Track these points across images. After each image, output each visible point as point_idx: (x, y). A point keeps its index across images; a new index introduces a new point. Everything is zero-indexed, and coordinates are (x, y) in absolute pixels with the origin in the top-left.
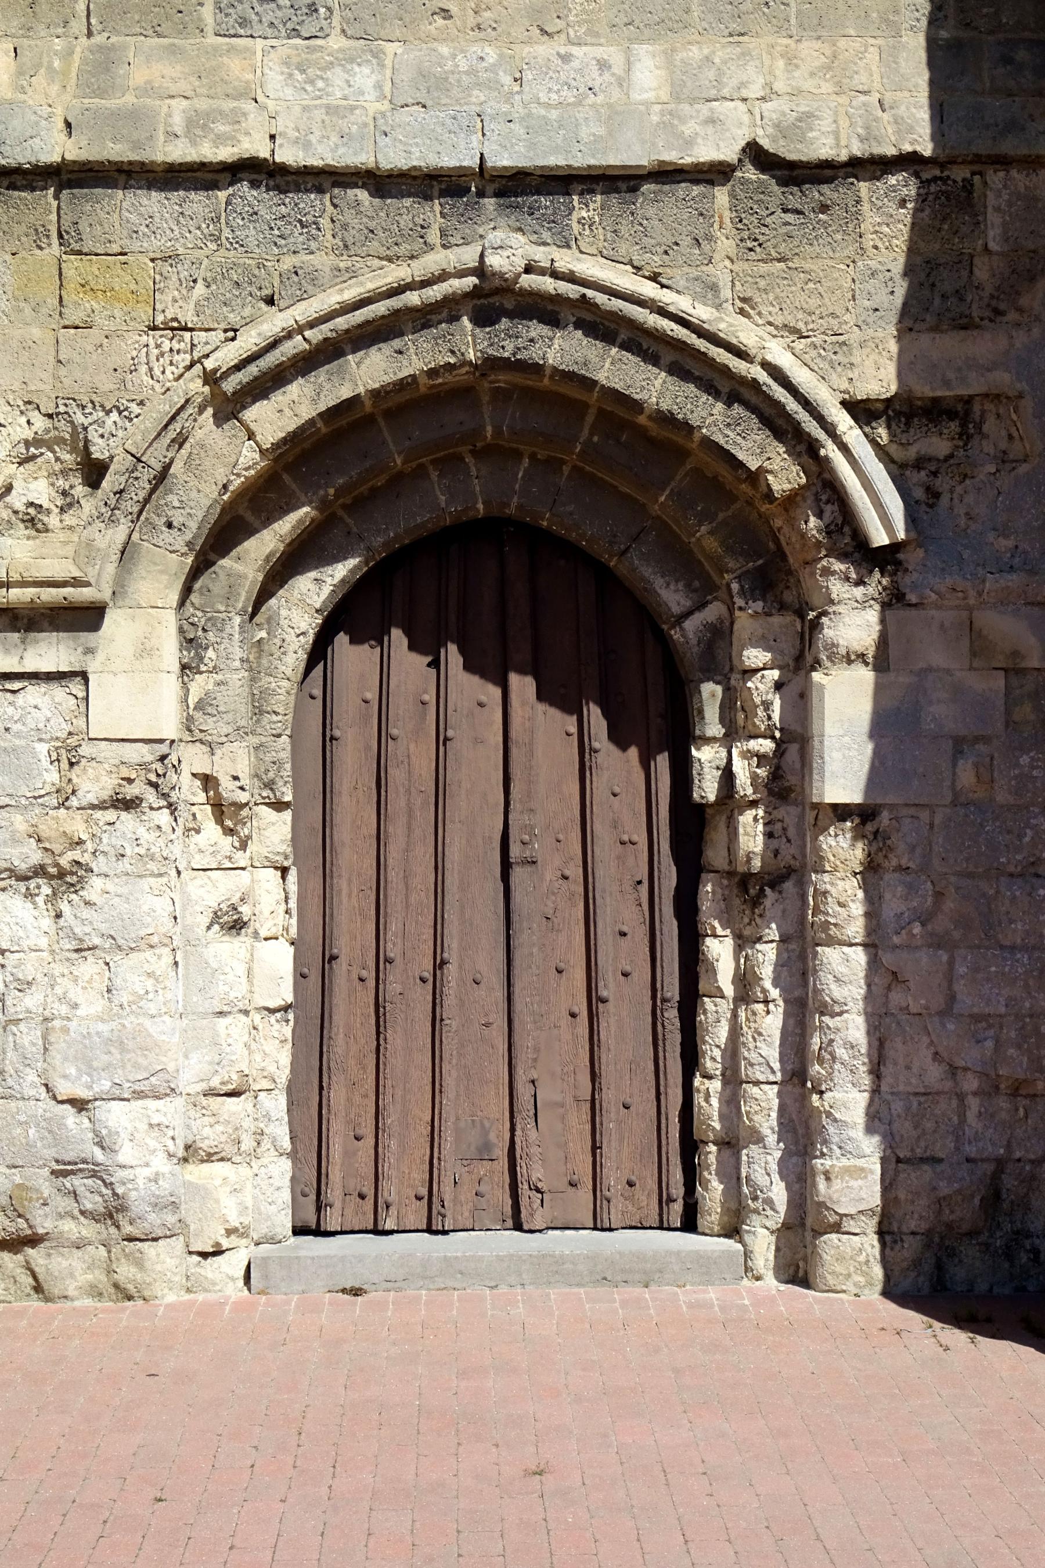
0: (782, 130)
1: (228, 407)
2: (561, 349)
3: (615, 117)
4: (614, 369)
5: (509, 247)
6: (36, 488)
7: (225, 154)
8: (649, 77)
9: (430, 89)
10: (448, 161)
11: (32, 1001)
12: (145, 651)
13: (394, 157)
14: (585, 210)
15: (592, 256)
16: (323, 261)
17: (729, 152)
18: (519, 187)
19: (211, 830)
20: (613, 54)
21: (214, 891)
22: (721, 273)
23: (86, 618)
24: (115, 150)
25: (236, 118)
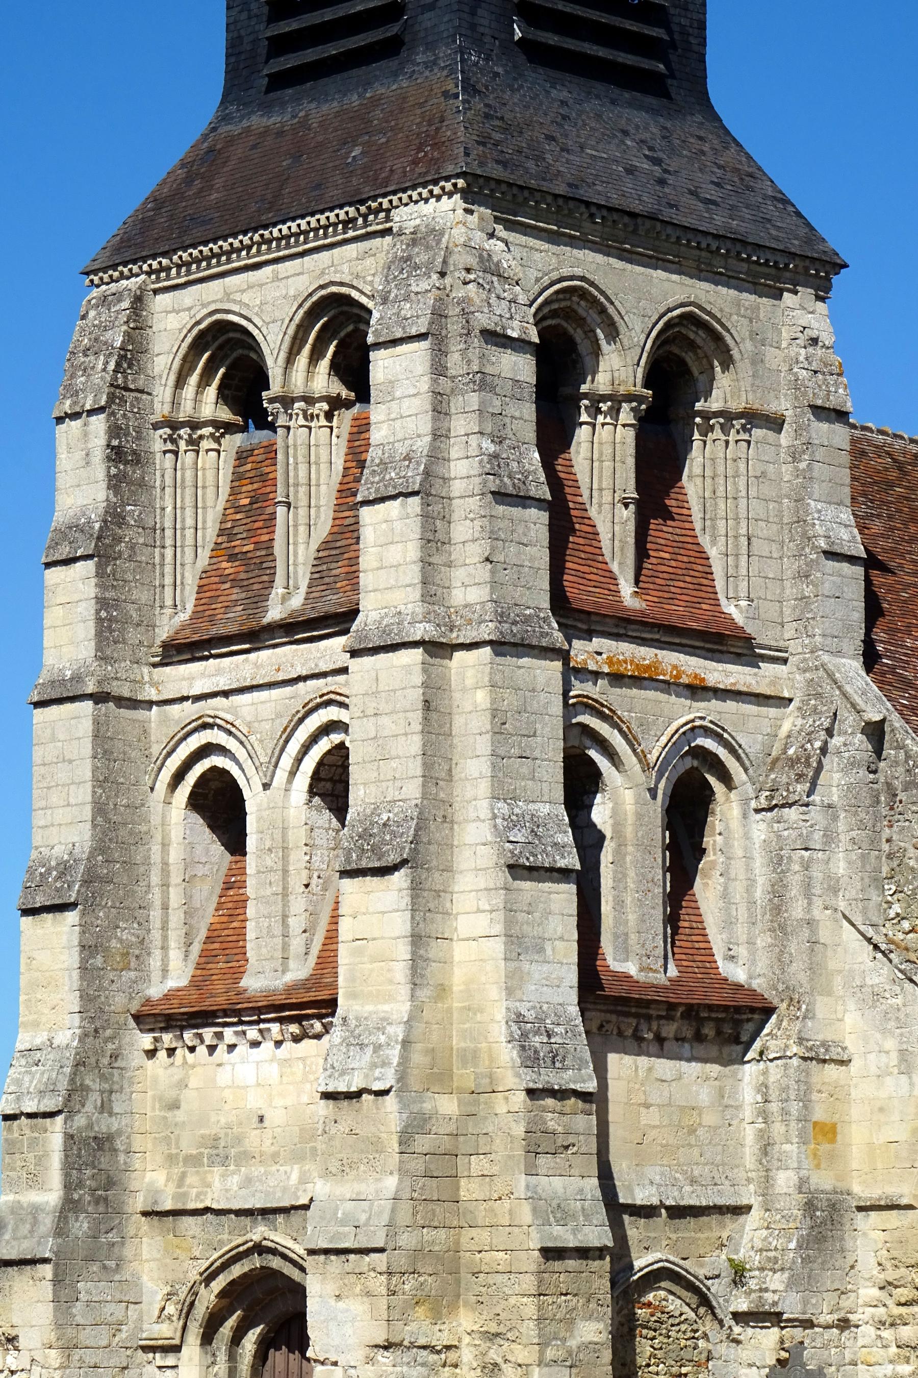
3: (285, 1189)
5: (259, 1232)
7: (201, 1206)
9: (248, 1182)
10: (247, 1207)
12: (190, 1359)
13: (236, 1206)
14: (280, 1219)
16: (226, 1237)
18: (266, 1212)
20: (288, 1168)
23: (177, 1349)
24: (179, 1206)
25: (206, 1194)
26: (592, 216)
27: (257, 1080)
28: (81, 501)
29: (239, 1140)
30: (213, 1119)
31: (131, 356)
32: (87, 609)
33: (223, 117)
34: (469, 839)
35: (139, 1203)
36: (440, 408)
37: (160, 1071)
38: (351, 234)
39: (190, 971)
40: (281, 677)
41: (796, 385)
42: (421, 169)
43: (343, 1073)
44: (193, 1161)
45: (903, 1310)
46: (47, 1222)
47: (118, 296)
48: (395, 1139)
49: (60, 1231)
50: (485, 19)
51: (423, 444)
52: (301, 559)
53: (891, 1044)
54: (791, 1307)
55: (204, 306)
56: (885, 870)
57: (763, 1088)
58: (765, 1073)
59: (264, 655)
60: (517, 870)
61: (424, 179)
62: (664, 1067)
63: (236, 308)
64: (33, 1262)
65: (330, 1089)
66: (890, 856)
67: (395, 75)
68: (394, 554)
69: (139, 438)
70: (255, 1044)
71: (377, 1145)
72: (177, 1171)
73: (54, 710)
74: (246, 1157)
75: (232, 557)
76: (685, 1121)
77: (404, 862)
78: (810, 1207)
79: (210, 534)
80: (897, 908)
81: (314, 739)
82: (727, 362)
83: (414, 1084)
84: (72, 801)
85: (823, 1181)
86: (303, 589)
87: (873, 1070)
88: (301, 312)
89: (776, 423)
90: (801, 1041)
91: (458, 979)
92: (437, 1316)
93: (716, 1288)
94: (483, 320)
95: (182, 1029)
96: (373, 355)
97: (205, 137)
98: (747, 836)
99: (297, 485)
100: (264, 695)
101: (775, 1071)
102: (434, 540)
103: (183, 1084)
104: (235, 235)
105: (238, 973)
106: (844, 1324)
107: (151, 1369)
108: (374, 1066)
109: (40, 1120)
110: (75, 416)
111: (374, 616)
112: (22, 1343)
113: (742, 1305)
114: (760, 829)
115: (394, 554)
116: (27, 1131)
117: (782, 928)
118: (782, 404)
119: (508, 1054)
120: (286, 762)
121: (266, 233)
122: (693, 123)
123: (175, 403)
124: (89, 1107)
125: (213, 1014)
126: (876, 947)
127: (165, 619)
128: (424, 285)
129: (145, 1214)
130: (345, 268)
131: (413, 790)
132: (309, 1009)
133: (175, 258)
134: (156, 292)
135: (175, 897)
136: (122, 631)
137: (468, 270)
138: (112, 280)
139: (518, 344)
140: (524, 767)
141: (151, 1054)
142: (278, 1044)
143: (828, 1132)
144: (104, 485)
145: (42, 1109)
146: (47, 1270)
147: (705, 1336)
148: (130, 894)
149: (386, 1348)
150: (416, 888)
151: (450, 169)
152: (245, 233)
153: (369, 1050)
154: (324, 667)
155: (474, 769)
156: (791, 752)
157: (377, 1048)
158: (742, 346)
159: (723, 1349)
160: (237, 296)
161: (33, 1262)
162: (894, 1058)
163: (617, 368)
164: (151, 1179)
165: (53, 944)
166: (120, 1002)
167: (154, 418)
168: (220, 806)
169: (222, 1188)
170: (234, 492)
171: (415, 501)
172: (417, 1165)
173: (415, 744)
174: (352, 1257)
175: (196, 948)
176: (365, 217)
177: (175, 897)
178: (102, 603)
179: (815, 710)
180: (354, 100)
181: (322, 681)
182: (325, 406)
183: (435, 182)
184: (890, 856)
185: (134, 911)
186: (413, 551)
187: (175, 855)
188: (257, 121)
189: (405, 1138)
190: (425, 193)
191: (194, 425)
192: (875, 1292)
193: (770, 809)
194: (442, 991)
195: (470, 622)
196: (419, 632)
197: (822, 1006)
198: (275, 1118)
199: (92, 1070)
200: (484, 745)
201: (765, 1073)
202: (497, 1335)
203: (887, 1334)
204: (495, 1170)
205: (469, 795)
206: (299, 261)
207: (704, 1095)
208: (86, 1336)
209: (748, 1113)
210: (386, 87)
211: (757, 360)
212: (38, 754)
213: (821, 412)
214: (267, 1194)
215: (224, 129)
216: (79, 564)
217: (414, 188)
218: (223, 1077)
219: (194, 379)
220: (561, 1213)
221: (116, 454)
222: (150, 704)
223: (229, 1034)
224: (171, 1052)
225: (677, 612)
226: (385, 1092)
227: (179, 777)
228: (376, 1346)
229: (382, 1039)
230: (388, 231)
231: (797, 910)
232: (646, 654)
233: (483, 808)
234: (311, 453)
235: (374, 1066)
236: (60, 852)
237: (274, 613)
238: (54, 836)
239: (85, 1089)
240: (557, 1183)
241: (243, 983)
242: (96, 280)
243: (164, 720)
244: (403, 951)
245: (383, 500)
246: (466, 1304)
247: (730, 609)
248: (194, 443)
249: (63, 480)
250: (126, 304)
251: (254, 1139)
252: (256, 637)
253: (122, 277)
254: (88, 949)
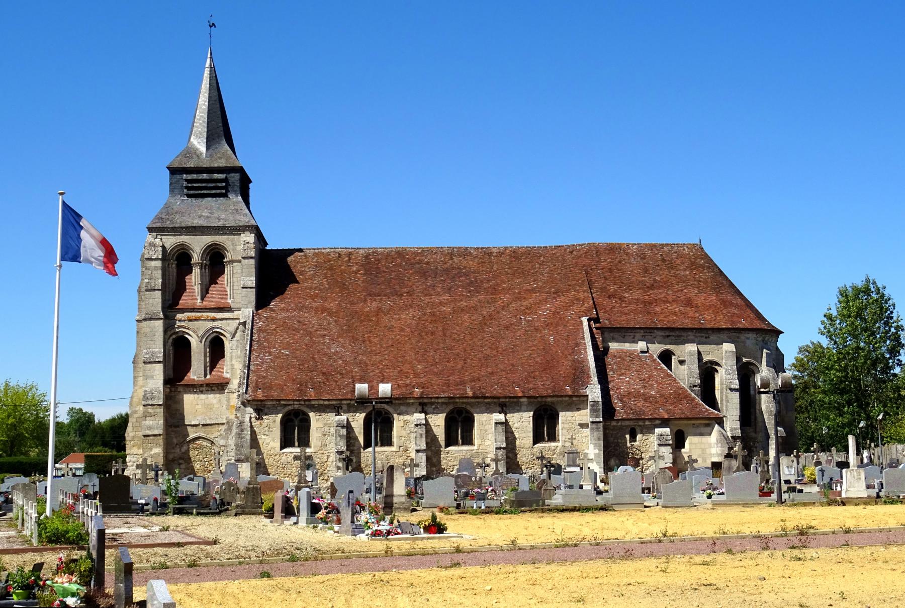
62: (202, 396)
76: (209, 407)
83: (134, 404)
207: (215, 401)
220: (150, 428)
232: (199, 314)
240: (151, 423)
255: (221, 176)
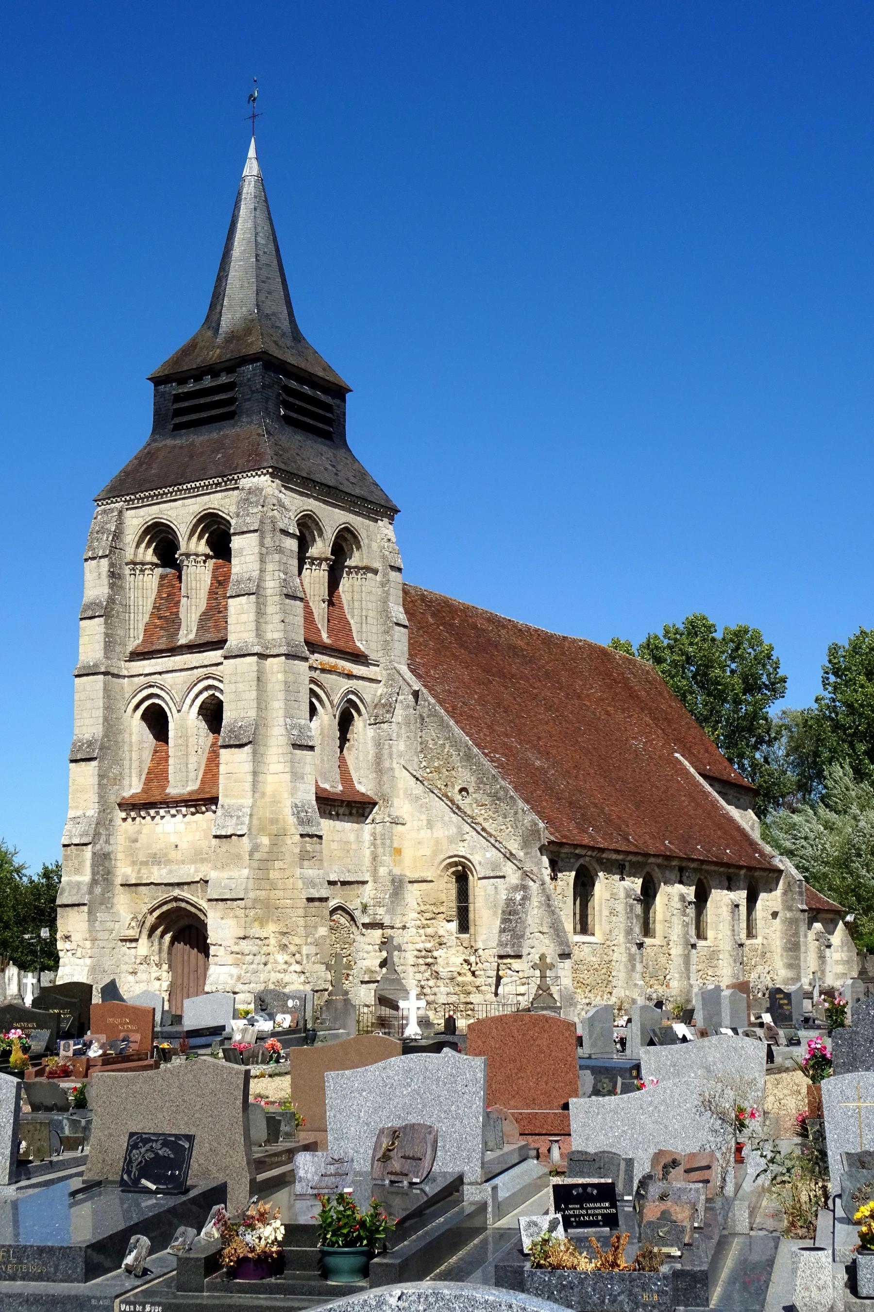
0: (205, 876)
1: (151, 912)
2: (183, 905)
3: (188, 875)
4: (189, 908)
5: (176, 892)
6: (133, 924)
8: (192, 868)
9: (170, 872)
11: (132, 989)
14: (186, 887)
15: (185, 893)
17: (197, 879)
18: (179, 885)
19: (155, 967)
21: (154, 975)
22: (199, 894)
23: (136, 940)
24: (139, 882)
26: (315, 486)
27: (174, 830)
28: (96, 593)
29: (166, 855)
30: (154, 846)
31: (117, 535)
32: (100, 638)
33: (153, 440)
34: (274, 734)
35: (119, 881)
36: (262, 561)
37: (129, 827)
38: (218, 489)
39: (141, 786)
40: (186, 667)
41: (384, 557)
42: (251, 464)
43: (223, 827)
44: (145, 863)
45: (428, 922)
46: (85, 889)
47: (112, 510)
48: (247, 854)
49: (90, 892)
50: (271, 405)
51: (256, 574)
52: (193, 619)
53: (424, 817)
54: (387, 921)
55: (150, 515)
56: (419, 749)
57: (374, 835)
58: (375, 828)
59: (178, 658)
60: (295, 746)
61: (255, 468)
63: (165, 517)
64: (78, 905)
65: (218, 834)
66: (421, 743)
67: (233, 426)
68: (244, 618)
69: (120, 568)
70: (174, 816)
71: (239, 857)
72: (137, 868)
73: (85, 678)
74: (169, 862)
75: (160, 618)
77: (250, 742)
78: (393, 881)
79: (149, 608)
80: (424, 764)
81: (200, 692)
82: (359, 547)
83: (254, 832)
84: (93, 715)
85: (397, 871)
86: (194, 631)
87: (416, 827)
88: (195, 520)
89: (375, 572)
90: (389, 816)
91: (269, 790)
92: (262, 926)
93: (357, 914)
94: (281, 525)
95: (140, 809)
96: (232, 538)
97: (145, 448)
98: (365, 734)
99: (191, 589)
100: (178, 674)
101: (379, 828)
102: (260, 613)
103: (139, 832)
104: (166, 488)
105: (164, 788)
106: (404, 927)
107: (125, 948)
108: (237, 824)
109: (80, 847)
110: (93, 558)
111: (234, 643)
112: (73, 938)
113: (367, 920)
114: (371, 732)
115: (244, 618)
116: (75, 851)
117: (380, 771)
118: (377, 565)
119: (292, 820)
120: (188, 701)
121: (180, 487)
122: (342, 453)
123: (135, 555)
124: (101, 841)
125: (155, 803)
126: (417, 779)
127: (131, 643)
128: (255, 510)
129: (122, 885)
130: (216, 502)
131: (252, 713)
132: (204, 801)
133: (137, 496)
134: (127, 509)
135: (135, 756)
136: (114, 647)
137: (274, 505)
138: (107, 503)
139: (292, 535)
140: (296, 704)
141: (124, 820)
142: (184, 816)
143: (398, 852)
144: (107, 587)
145: (82, 842)
146: (86, 908)
147: (353, 933)
148: (117, 754)
149: (244, 939)
150: (254, 753)
151: (265, 465)
152: (170, 487)
153: (235, 819)
154: (206, 663)
155: (277, 706)
156: (383, 701)
157: (238, 817)
158: (364, 542)
159: (359, 938)
160: (166, 512)
161: (78, 905)
162: (425, 823)
163: (321, 548)
164: (124, 871)
165: (85, 775)
166: (113, 799)
167: (126, 561)
168: (157, 720)
169: (158, 874)
170: (159, 592)
171: (254, 596)
172: (255, 865)
173: (254, 695)
174: (229, 902)
175: (144, 777)
176: (226, 482)
177: (135, 756)
178: (107, 635)
179: (391, 685)
180: (215, 435)
181: (205, 669)
182: (204, 558)
183: (259, 469)
184: (421, 743)
185: (117, 761)
186: (252, 617)
187: (134, 739)
188: (170, 442)
189: (251, 854)
190: (254, 474)
191: (143, 564)
192: (417, 915)
193: (376, 724)
194: (263, 794)
195: (275, 646)
196: (257, 649)
197: (396, 802)
198: (183, 846)
199: (102, 826)
200: (281, 695)
201: (375, 828)
202: (286, 933)
203: (422, 931)
204: (286, 866)
205: (274, 716)
206: (194, 499)
207: (352, 837)
208: (100, 935)
209: (367, 844)
210: (229, 431)
211: (369, 547)
212: (77, 696)
213: (393, 568)
214: (180, 877)
215: (154, 445)
216: (96, 619)
217: (249, 471)
218: (159, 829)
219: (143, 545)
221: (112, 575)
222: (124, 677)
223: (162, 812)
224: (134, 819)
225: (341, 644)
226: (243, 835)
227: (137, 707)
228: (240, 938)
229: (241, 814)
230: (238, 488)
231: (387, 764)
232: (332, 661)
233: (281, 721)
234: (198, 576)
235: (237, 824)
236: (88, 737)
237: (182, 641)
238: (84, 730)
239: (100, 834)
240: (310, 872)
241: (167, 791)
242: (100, 503)
243: (131, 684)
244: (250, 778)
245: (239, 596)
246: (272, 920)
247: (358, 644)
248: (142, 571)
249: (87, 585)
250: (116, 513)
251: (173, 854)
252: (174, 651)
253: (112, 502)
254: (101, 776)
255: (328, 400)
